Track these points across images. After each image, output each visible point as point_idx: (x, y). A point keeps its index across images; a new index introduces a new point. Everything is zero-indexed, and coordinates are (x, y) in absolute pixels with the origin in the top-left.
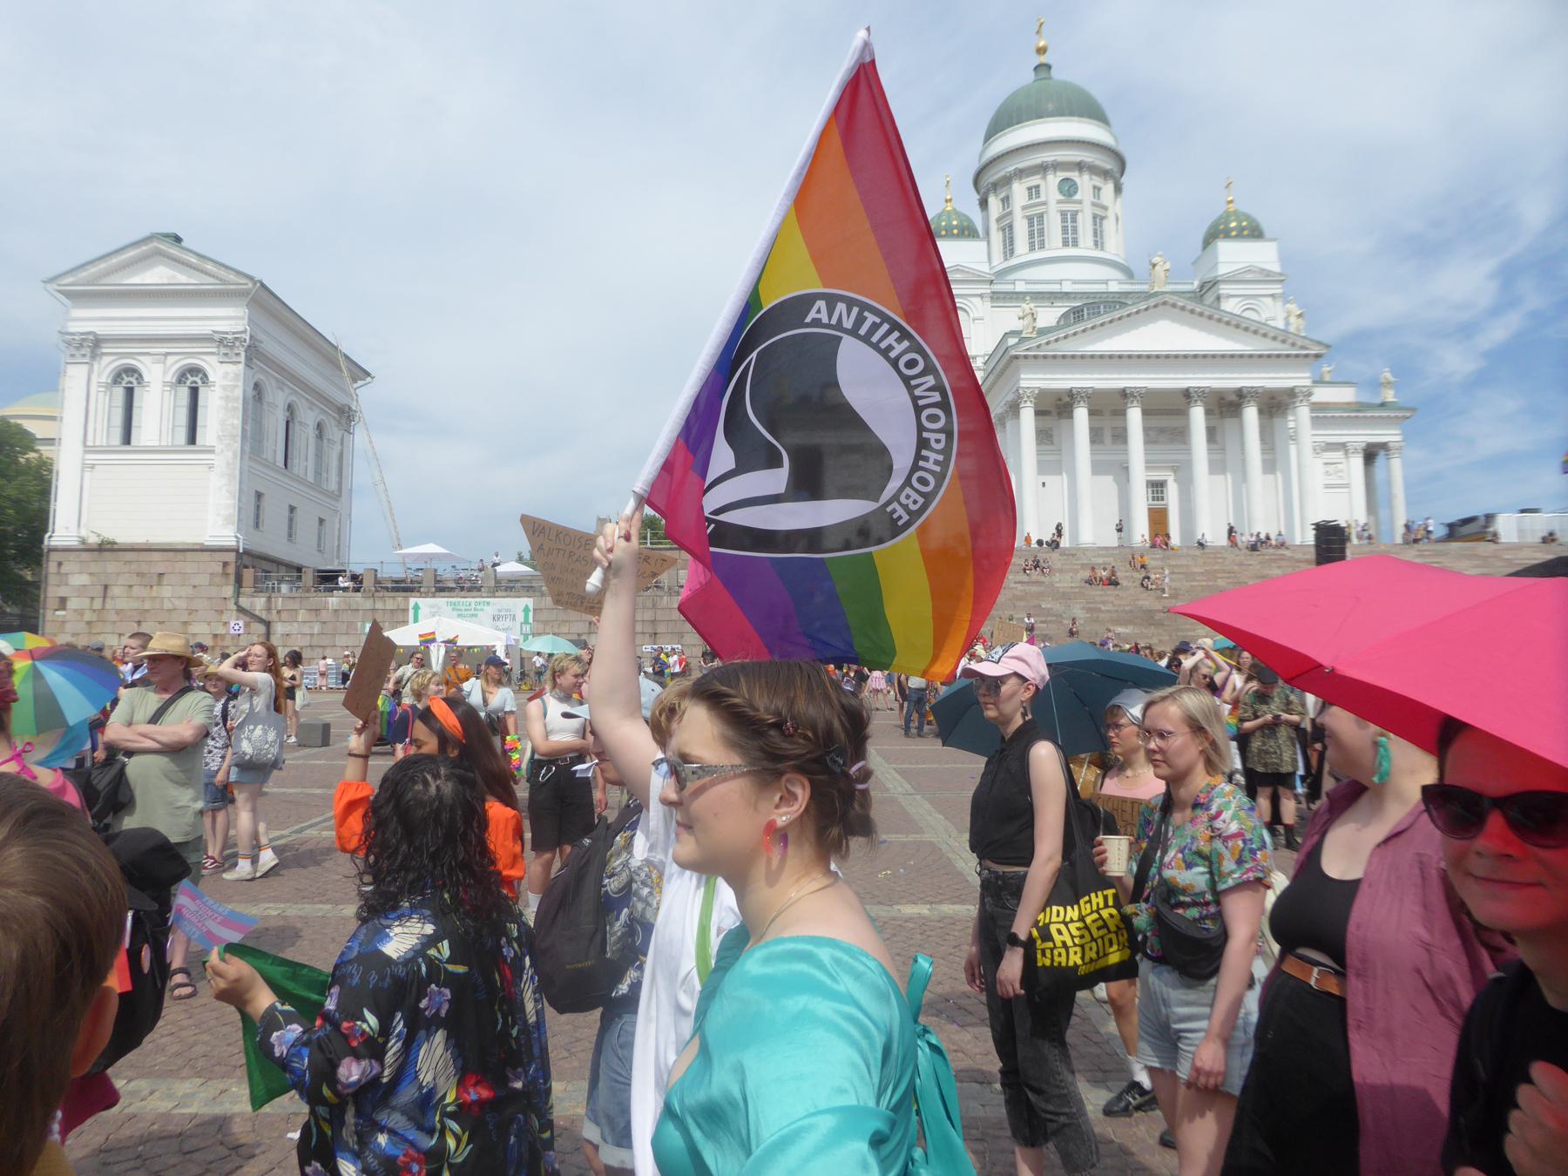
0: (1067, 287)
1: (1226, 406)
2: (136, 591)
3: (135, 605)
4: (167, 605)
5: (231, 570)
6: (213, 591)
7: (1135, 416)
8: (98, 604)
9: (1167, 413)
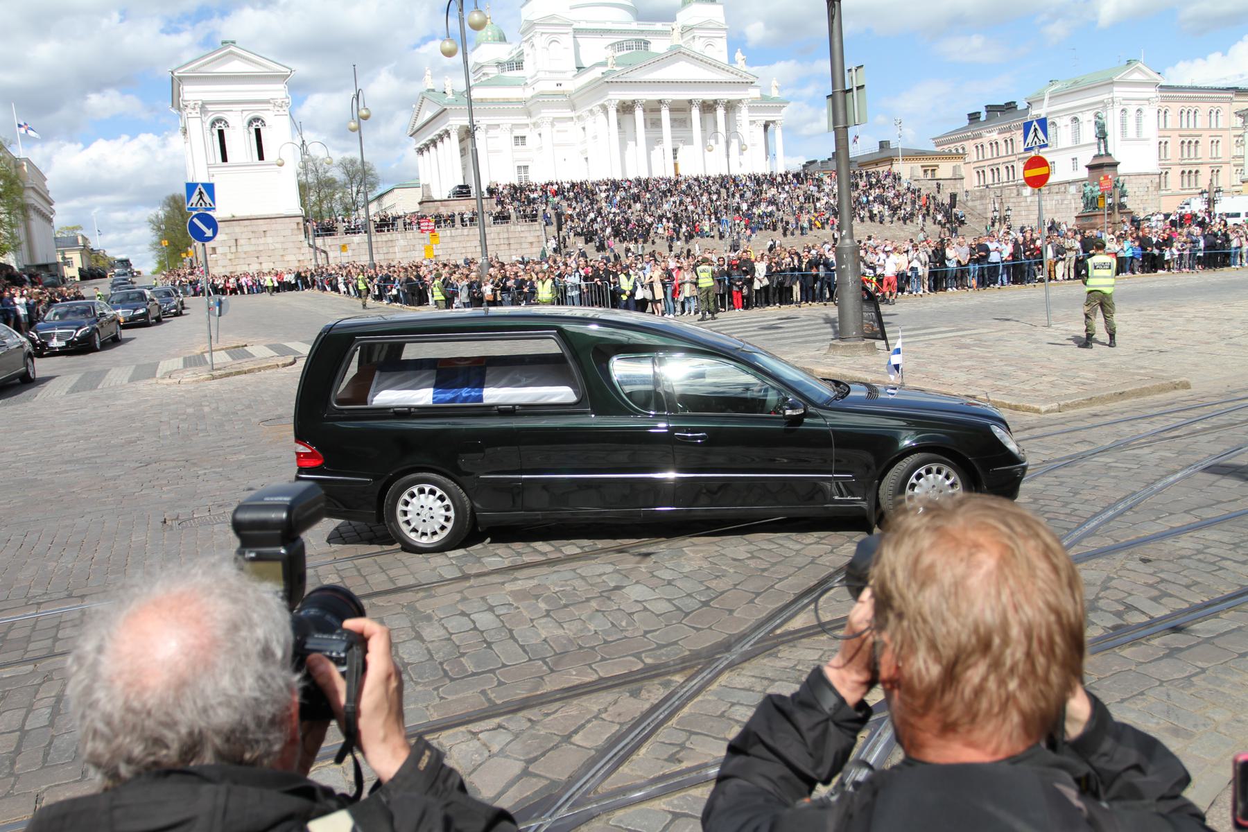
0: (609, 26)
1: (708, 107)
2: (253, 241)
3: (253, 248)
4: (272, 247)
5: (302, 226)
6: (294, 238)
7: (665, 114)
8: (233, 249)
9: (680, 111)
